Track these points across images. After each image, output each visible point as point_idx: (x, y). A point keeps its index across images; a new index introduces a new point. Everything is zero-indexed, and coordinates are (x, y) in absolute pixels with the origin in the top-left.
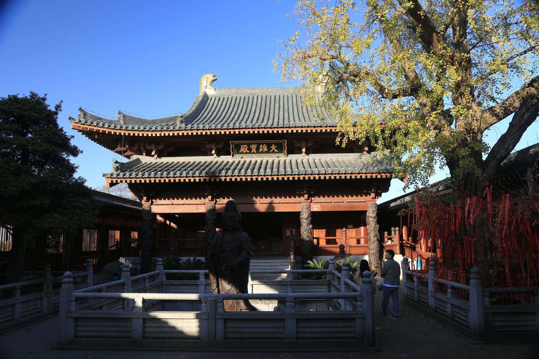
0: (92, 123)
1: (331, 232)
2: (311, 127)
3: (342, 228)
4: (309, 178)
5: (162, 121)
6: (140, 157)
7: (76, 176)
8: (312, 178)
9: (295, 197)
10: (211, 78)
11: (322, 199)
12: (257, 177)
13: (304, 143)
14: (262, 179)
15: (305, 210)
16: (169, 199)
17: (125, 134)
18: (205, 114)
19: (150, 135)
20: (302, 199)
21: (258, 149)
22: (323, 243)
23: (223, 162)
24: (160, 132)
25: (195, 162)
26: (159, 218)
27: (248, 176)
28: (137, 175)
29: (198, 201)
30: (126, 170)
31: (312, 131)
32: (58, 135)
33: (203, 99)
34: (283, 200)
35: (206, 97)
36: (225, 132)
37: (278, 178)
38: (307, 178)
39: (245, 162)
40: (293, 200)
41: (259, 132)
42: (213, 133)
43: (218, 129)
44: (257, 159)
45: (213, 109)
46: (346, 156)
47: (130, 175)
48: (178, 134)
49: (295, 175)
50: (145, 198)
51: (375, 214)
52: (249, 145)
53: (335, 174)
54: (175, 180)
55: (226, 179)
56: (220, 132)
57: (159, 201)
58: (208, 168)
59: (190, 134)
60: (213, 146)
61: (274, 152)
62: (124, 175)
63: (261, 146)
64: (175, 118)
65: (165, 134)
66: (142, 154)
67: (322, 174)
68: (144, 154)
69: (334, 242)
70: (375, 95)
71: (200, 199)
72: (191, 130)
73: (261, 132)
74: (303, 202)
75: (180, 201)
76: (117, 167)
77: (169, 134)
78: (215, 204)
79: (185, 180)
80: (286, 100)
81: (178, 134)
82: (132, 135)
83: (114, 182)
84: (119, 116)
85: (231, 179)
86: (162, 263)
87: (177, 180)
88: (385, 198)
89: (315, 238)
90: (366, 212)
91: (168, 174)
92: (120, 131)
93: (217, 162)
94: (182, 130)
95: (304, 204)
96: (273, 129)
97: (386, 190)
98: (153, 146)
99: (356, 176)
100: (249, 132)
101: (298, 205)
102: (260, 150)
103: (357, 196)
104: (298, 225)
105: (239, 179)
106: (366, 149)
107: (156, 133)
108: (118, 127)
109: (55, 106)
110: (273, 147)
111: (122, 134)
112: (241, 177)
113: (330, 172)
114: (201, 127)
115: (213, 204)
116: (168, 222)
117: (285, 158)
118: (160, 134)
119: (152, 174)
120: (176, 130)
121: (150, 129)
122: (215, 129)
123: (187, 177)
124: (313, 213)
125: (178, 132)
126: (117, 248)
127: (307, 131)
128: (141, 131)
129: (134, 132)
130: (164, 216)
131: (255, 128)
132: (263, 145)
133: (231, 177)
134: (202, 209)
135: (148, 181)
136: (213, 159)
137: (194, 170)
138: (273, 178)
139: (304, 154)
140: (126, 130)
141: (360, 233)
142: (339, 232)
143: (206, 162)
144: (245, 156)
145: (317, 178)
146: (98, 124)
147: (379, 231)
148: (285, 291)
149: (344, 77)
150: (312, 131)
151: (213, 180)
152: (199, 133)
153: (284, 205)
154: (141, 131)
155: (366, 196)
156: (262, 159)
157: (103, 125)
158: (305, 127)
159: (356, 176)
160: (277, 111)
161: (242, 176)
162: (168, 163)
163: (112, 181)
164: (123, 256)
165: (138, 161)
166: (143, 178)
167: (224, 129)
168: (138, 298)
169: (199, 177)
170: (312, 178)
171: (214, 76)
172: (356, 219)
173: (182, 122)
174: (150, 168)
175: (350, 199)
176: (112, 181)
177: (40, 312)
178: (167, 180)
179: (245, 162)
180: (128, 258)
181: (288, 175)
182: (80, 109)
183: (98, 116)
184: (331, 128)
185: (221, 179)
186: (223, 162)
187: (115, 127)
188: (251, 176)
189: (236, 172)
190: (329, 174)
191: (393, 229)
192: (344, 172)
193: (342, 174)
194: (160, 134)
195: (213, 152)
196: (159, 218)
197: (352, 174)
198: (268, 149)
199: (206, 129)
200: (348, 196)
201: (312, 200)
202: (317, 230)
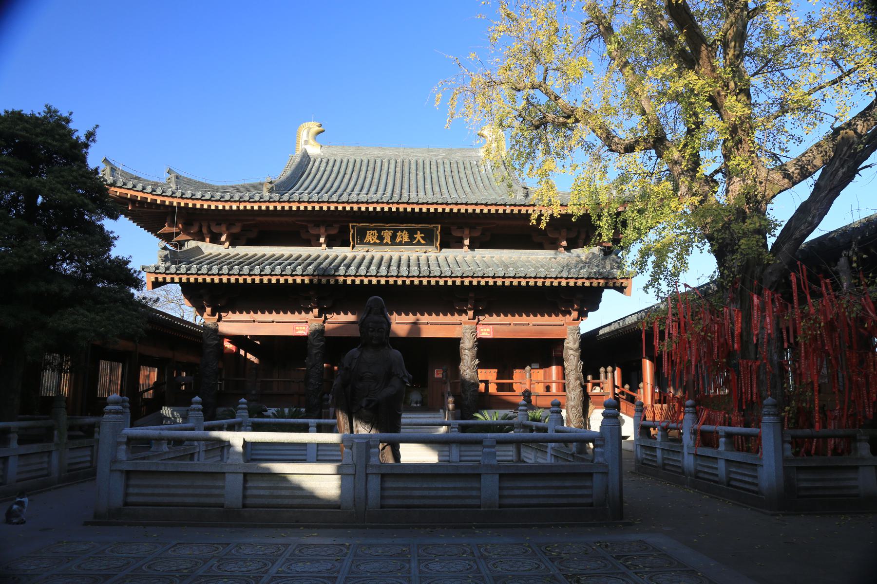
0: (125, 184)
1: (505, 372)
2: (482, 204)
3: (524, 368)
4: (479, 282)
5: (238, 188)
6: (201, 244)
8: (483, 283)
9: (453, 315)
10: (316, 129)
11: (494, 319)
12: (395, 279)
13: (467, 232)
14: (404, 282)
15: (468, 335)
16: (248, 313)
17: (179, 203)
18: (306, 182)
19: (220, 207)
20: (464, 318)
21: (393, 237)
22: (493, 389)
23: (337, 257)
24: (238, 204)
25: (291, 256)
26: (228, 345)
27: (382, 276)
28: (199, 270)
29: (296, 317)
30: (180, 262)
31: (482, 210)
32: (91, 179)
33: (301, 160)
34: (434, 318)
35: (306, 158)
36: (344, 208)
37: (429, 282)
38: (475, 283)
39: (373, 258)
40: (449, 318)
41: (398, 209)
42: (325, 208)
43: (333, 202)
44: (392, 254)
45: (318, 177)
46: (532, 254)
47: (188, 269)
48: (268, 207)
49: (457, 277)
50: (209, 310)
51: (577, 345)
52: (379, 231)
53: (520, 277)
54: (261, 280)
55: (345, 281)
56: (336, 208)
57: (231, 316)
58: (315, 263)
59: (287, 208)
61: (419, 244)
62: (178, 269)
63: (399, 234)
64: (260, 186)
65: (245, 207)
66: (203, 240)
67: (499, 277)
68: (208, 240)
69: (510, 388)
70: (595, 149)
71: (300, 313)
72: (289, 202)
73: (401, 210)
74: (465, 323)
75: (267, 317)
76: (166, 256)
77: (252, 207)
78: (324, 322)
79: (278, 280)
80: (434, 167)
81: (268, 207)
82: (190, 206)
83: (160, 280)
84: (169, 176)
85: (353, 281)
86: (245, 406)
87: (265, 280)
89: (482, 381)
90: (563, 340)
91: (251, 270)
92: (171, 199)
93: (327, 257)
94: (274, 202)
95: (467, 326)
96: (420, 206)
97: (595, 307)
98: (223, 228)
99: (552, 283)
100: (382, 209)
101: (458, 328)
102: (398, 240)
103: (550, 316)
104: (456, 358)
105: (366, 282)
106: (564, 243)
107: (230, 204)
108: (169, 193)
109: (85, 132)
110: (419, 236)
111: (175, 204)
112: (370, 278)
113: (512, 275)
114: (305, 197)
115: (321, 323)
116: (242, 352)
117: (438, 254)
118: (238, 207)
119: (225, 269)
120: (265, 202)
121: (222, 197)
122: (328, 202)
123: (281, 275)
124: (480, 340)
125: (267, 204)
126: (154, 394)
127: (474, 210)
128: (207, 200)
129: (195, 202)
130: (239, 340)
131: (393, 203)
133: (353, 278)
134: (302, 331)
135: (216, 280)
136: (321, 251)
137: (294, 265)
138: (421, 282)
139: (466, 248)
140: (181, 197)
141: (550, 376)
142: (517, 373)
143: (310, 256)
144: (372, 248)
145: (491, 283)
146: (134, 186)
147: (583, 372)
148: (447, 453)
149: (548, 119)
150: (482, 210)
151: (324, 281)
152: (302, 208)
153: (435, 326)
154: (207, 200)
155: (564, 315)
156: (400, 254)
157: (144, 188)
158: (472, 204)
159: (552, 283)
160: (421, 183)
161: (371, 276)
162: (247, 255)
163: (157, 279)
164: (169, 406)
165: (198, 250)
166: (209, 275)
167: (343, 203)
168: (237, 439)
169: (302, 275)
170: (483, 283)
171: (320, 126)
172: (546, 352)
173: (271, 191)
174: (220, 260)
175: (539, 320)
176: (157, 279)
177: (47, 475)
178: (249, 280)
179: (373, 258)
180: (176, 408)
181: (446, 277)
183: (134, 174)
184: (513, 208)
185: (337, 281)
186: (337, 257)
187: (163, 192)
188: (387, 276)
189: (362, 270)
190: (509, 277)
191: (602, 370)
192: (533, 276)
193: (530, 278)
194: (238, 207)
195: (322, 240)
196: (228, 345)
197: (545, 278)
198: (409, 238)
199: (313, 202)
200: (535, 316)
201: (479, 320)
202: (484, 371)
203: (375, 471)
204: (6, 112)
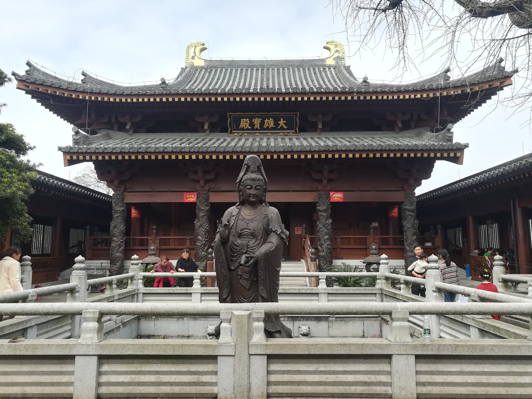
13: (320, 116)
21: (262, 124)
66: (112, 129)
68: (116, 128)
83: (75, 157)
88: (425, 187)
97: (427, 175)
106: (400, 125)
110: (282, 122)
132: (269, 119)
163: (71, 157)
182: (28, 64)
183: (53, 74)
195: (206, 127)
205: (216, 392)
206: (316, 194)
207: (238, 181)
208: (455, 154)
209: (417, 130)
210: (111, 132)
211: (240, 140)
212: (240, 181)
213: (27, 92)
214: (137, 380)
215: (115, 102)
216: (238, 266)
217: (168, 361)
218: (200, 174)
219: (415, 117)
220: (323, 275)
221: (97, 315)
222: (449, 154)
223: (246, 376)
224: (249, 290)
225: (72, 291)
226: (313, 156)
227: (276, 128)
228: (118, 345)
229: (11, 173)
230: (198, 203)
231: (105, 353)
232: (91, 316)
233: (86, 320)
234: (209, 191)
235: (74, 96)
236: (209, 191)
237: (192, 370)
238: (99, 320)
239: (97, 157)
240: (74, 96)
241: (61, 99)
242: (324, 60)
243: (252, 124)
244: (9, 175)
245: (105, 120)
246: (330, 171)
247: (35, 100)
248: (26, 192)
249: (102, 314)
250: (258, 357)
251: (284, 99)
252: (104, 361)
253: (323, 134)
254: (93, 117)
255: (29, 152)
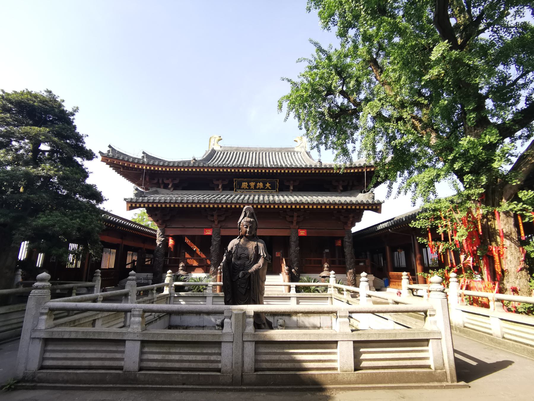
7: (88, 181)
13: (292, 182)
21: (255, 186)
60: (220, 181)
63: (258, 184)
66: (160, 187)
68: (162, 187)
88: (357, 228)
97: (359, 220)
102: (257, 188)
106: (341, 188)
110: (268, 185)
163: (132, 205)
182: (110, 146)
183: (124, 153)
195: (220, 187)
203: (250, 339)
204: (15, 92)
205: (220, 367)
206: (288, 230)
207: (239, 222)
208: (376, 207)
209: (352, 191)
210: (158, 189)
211: (241, 195)
212: (240, 223)
213: (107, 164)
214: (166, 358)
215: (162, 171)
216: (238, 279)
217: (188, 345)
218: (215, 217)
219: (351, 184)
220: (293, 285)
221: (141, 313)
222: (372, 207)
223: (241, 356)
224: (245, 295)
225: (126, 295)
226: (287, 207)
227: (264, 188)
228: (155, 333)
229: (92, 215)
230: (213, 236)
231: (146, 339)
232: (137, 313)
233: (134, 316)
234: (220, 228)
235: (136, 166)
236: (220, 228)
237: (204, 352)
238: (142, 317)
239: (148, 205)
240: (136, 166)
241: (128, 168)
242: (293, 148)
243: (249, 186)
244: (91, 217)
245: (156, 181)
246: (298, 216)
247: (112, 169)
248: (100, 228)
249: (145, 311)
250: (249, 343)
251: (269, 171)
252: (145, 344)
253: (294, 193)
254: (147, 179)
255: (104, 202)
